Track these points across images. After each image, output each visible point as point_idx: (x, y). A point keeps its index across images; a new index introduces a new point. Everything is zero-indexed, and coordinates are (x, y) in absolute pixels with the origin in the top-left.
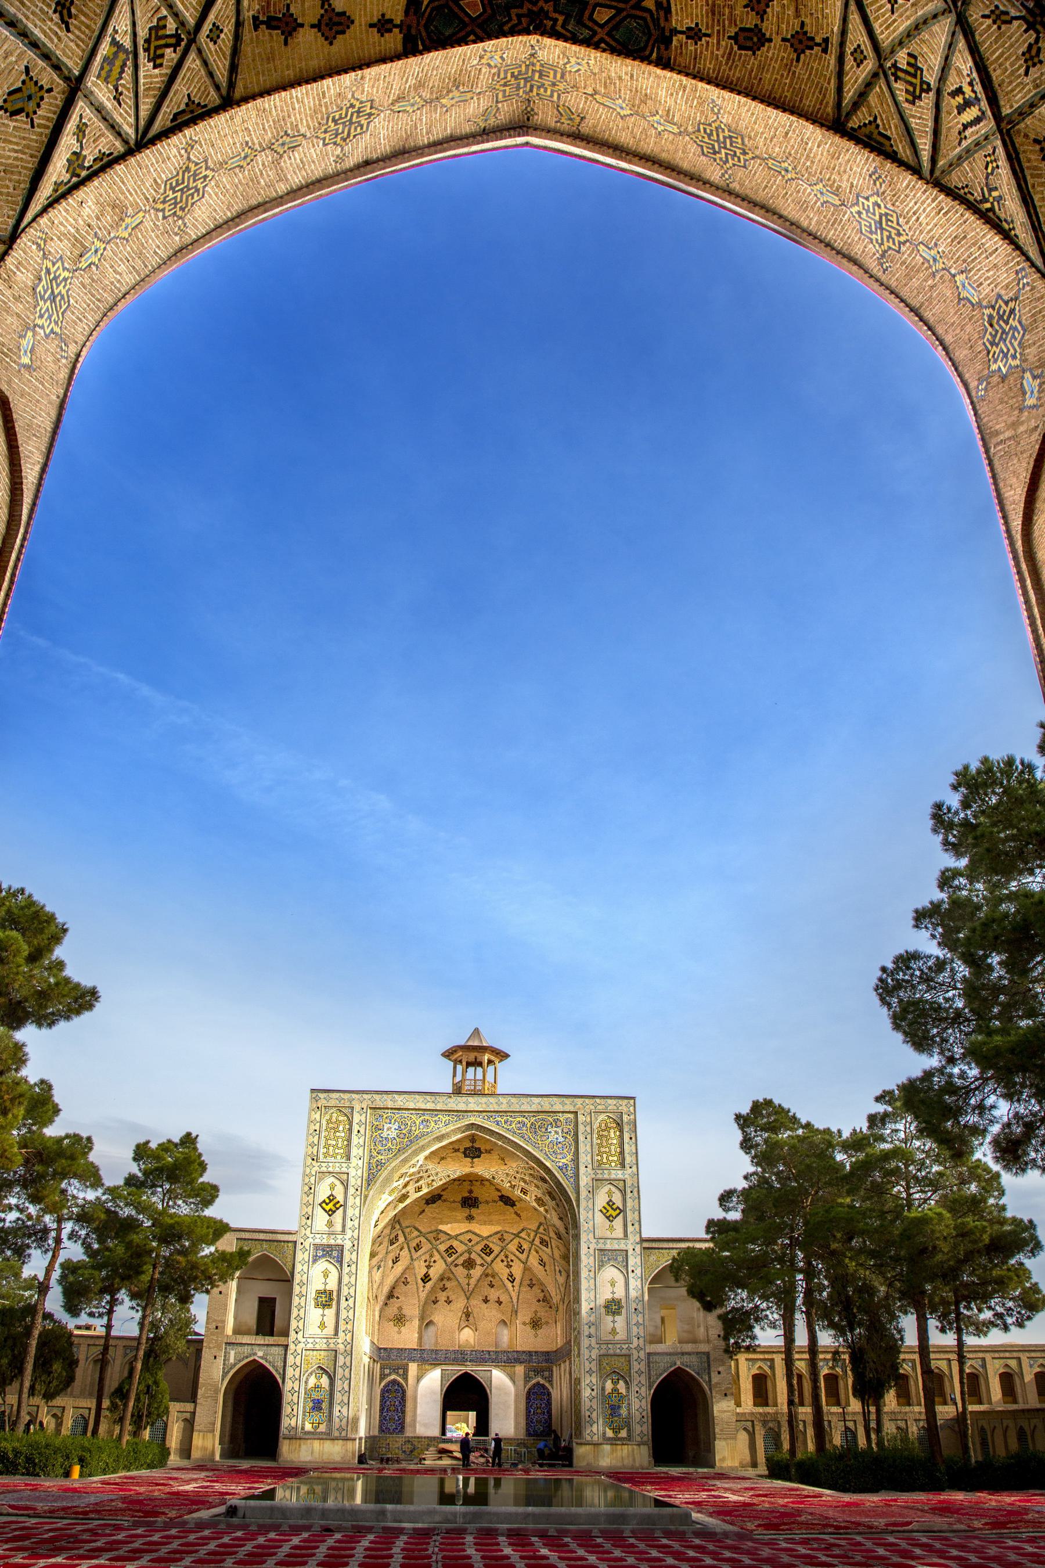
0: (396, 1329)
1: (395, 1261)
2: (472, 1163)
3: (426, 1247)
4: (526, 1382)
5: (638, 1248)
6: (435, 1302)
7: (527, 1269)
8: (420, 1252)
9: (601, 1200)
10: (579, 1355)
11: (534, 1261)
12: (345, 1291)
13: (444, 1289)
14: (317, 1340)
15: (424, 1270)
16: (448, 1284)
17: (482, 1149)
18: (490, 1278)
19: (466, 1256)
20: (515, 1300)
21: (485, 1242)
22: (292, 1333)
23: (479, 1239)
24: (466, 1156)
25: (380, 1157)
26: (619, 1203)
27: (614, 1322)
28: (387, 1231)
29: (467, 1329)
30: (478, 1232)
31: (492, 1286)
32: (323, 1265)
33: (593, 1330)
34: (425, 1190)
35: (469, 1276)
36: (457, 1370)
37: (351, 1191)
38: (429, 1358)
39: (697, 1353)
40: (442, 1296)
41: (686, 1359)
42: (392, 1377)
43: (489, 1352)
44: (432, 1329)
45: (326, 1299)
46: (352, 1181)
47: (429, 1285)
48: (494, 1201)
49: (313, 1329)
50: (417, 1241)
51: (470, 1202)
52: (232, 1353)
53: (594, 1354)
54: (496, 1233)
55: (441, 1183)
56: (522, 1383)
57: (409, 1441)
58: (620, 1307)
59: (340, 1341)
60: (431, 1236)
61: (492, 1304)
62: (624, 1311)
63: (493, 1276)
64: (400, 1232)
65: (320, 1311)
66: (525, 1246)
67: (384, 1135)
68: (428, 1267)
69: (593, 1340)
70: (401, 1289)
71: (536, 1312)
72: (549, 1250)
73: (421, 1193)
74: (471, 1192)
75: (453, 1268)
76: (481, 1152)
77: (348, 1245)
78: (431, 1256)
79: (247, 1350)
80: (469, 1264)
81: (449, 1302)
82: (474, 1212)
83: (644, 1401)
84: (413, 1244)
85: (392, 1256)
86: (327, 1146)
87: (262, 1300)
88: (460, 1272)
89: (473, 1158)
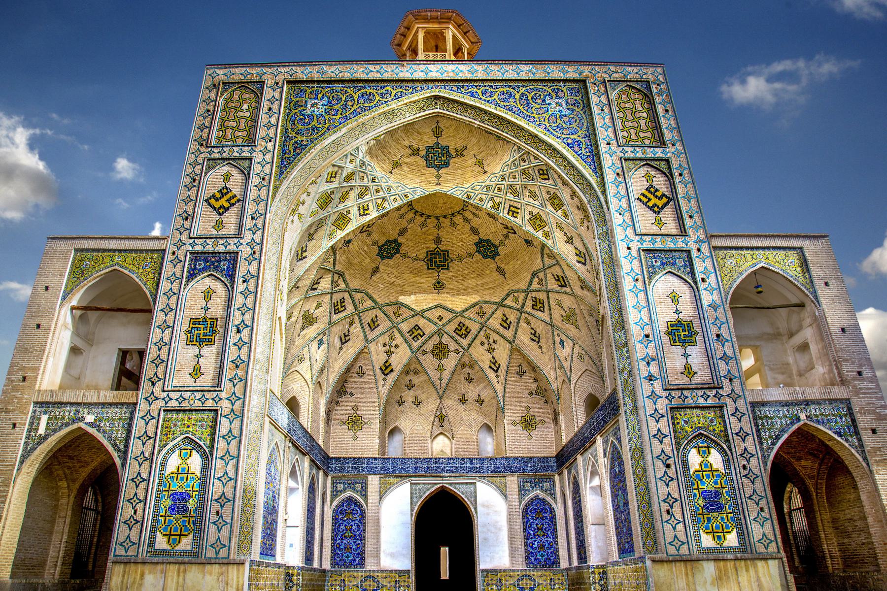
0: (351, 433)
1: (345, 339)
2: (438, 177)
3: (384, 325)
4: (521, 496)
5: (705, 248)
6: (400, 403)
7: (516, 351)
8: (377, 332)
9: (637, 182)
10: (635, 409)
11: (523, 337)
12: (237, 318)
13: (410, 386)
14: (187, 395)
15: (383, 358)
16: (416, 380)
17: (453, 153)
18: (467, 365)
19: (436, 339)
20: (500, 395)
21: (460, 319)
22: (145, 385)
23: (451, 315)
24: (429, 166)
25: (299, 138)
26: (663, 189)
27: (686, 356)
28: (325, 284)
29: (441, 437)
30: (450, 306)
31: (469, 380)
32: (204, 282)
33: (654, 369)
34: (374, 214)
35: (441, 368)
36: (430, 486)
37: (255, 180)
38: (394, 469)
39: (831, 401)
40: (409, 396)
41: (813, 410)
42: (349, 493)
43: (471, 460)
44: (398, 438)
45: (204, 332)
46: (256, 168)
47: (391, 378)
48: (470, 255)
49: (181, 378)
50: (371, 315)
51: (438, 260)
52: (44, 418)
53: (662, 405)
54: (474, 305)
55: (396, 205)
56: (515, 497)
57: (370, 576)
58: (692, 334)
59: (223, 395)
60: (390, 310)
61: (471, 404)
62: (699, 338)
63: (471, 367)
64: (346, 295)
65: (195, 350)
66: (512, 318)
67: (308, 111)
68: (389, 353)
69: (658, 386)
70: (354, 382)
71: (528, 409)
72: (545, 316)
73: (368, 218)
74: (438, 241)
75: (419, 355)
76: (450, 156)
77: (245, 251)
78: (392, 338)
79: (68, 413)
80: (441, 351)
81: (417, 403)
82: (444, 275)
83: (758, 481)
84: (367, 318)
85: (337, 330)
86: (223, 128)
87: (124, 354)
88: (429, 362)
89: (439, 167)
